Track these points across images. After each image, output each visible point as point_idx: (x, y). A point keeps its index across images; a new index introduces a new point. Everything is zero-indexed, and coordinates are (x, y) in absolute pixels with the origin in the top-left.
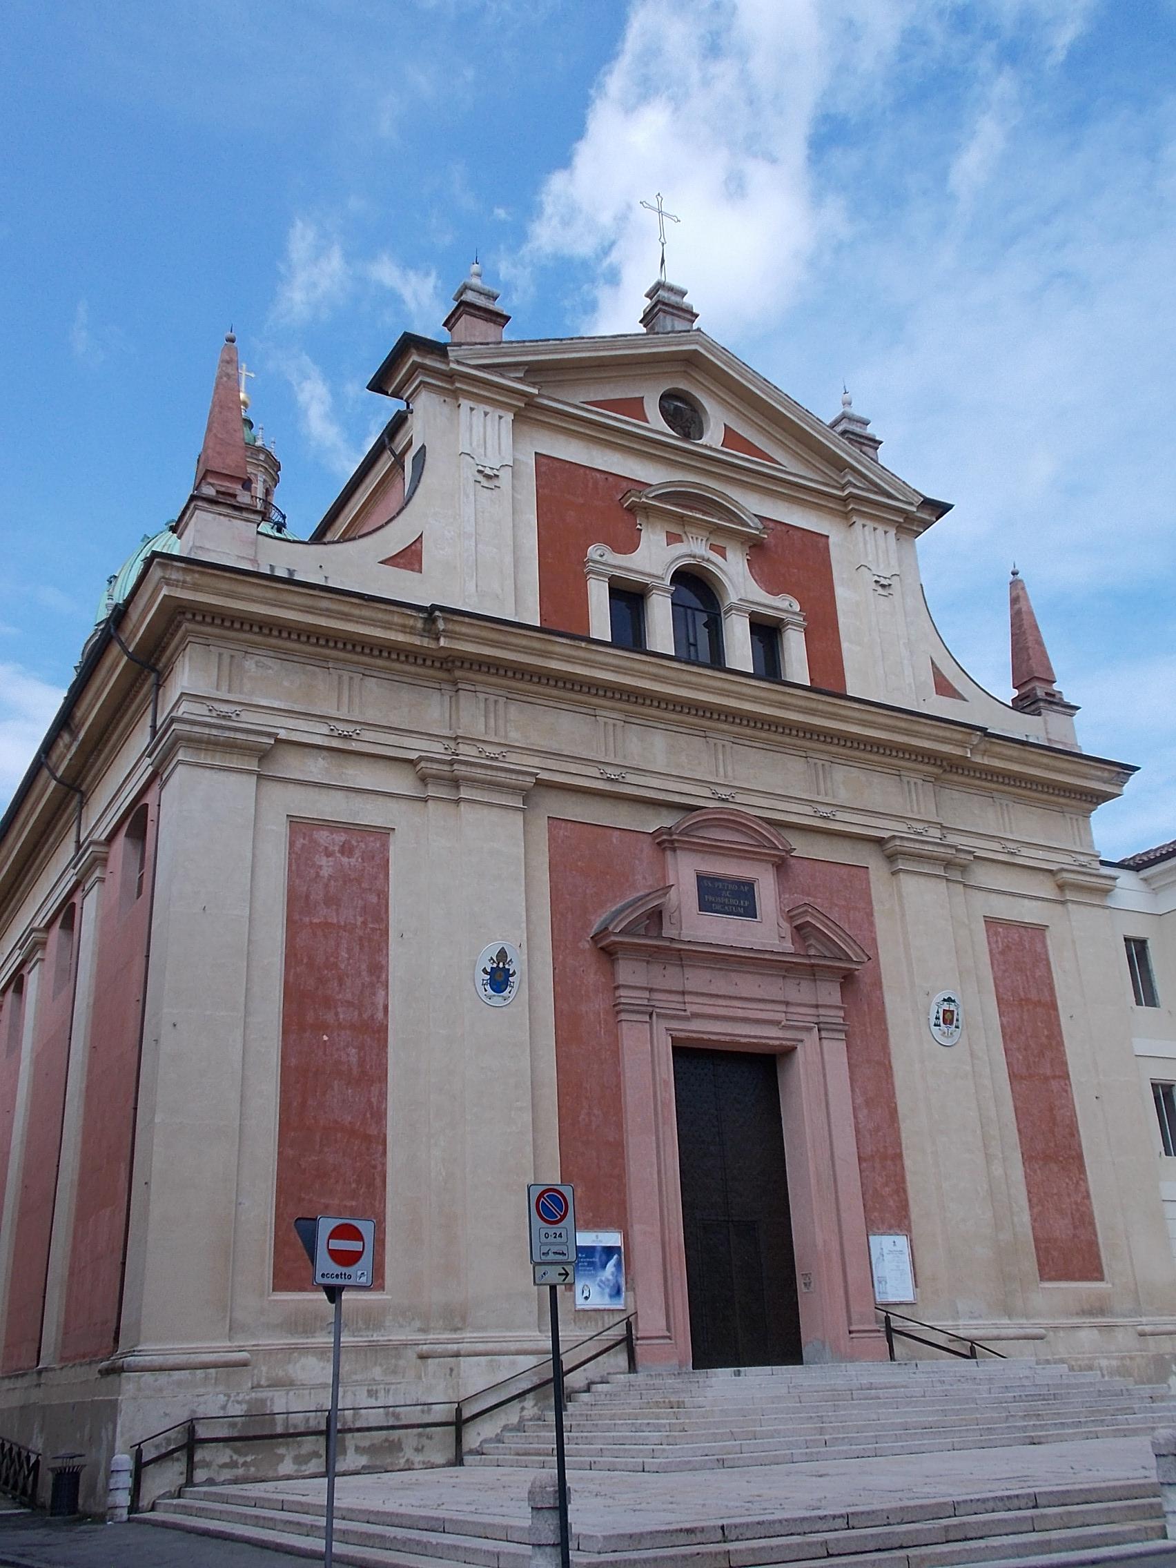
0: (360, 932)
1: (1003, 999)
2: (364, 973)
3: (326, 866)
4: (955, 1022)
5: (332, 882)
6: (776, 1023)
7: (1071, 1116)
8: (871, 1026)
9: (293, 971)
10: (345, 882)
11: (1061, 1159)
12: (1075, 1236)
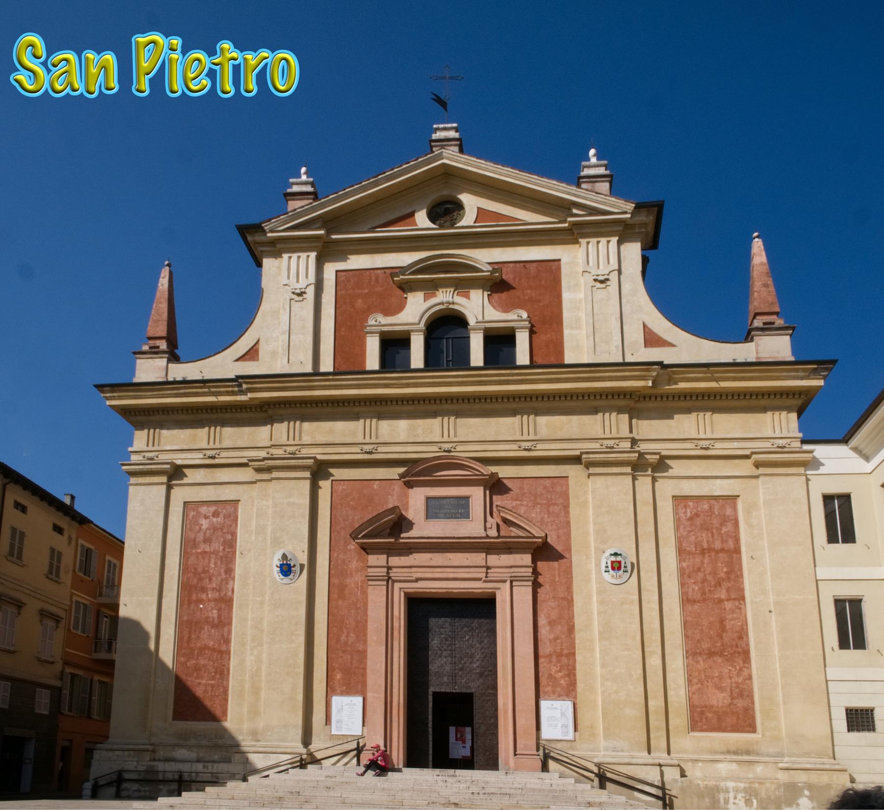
0: (221, 554)
1: (685, 550)
2: (223, 574)
3: (205, 524)
4: (623, 568)
5: (208, 532)
7: (742, 625)
8: (559, 576)
9: (186, 576)
10: (214, 531)
11: (726, 654)
12: (730, 704)
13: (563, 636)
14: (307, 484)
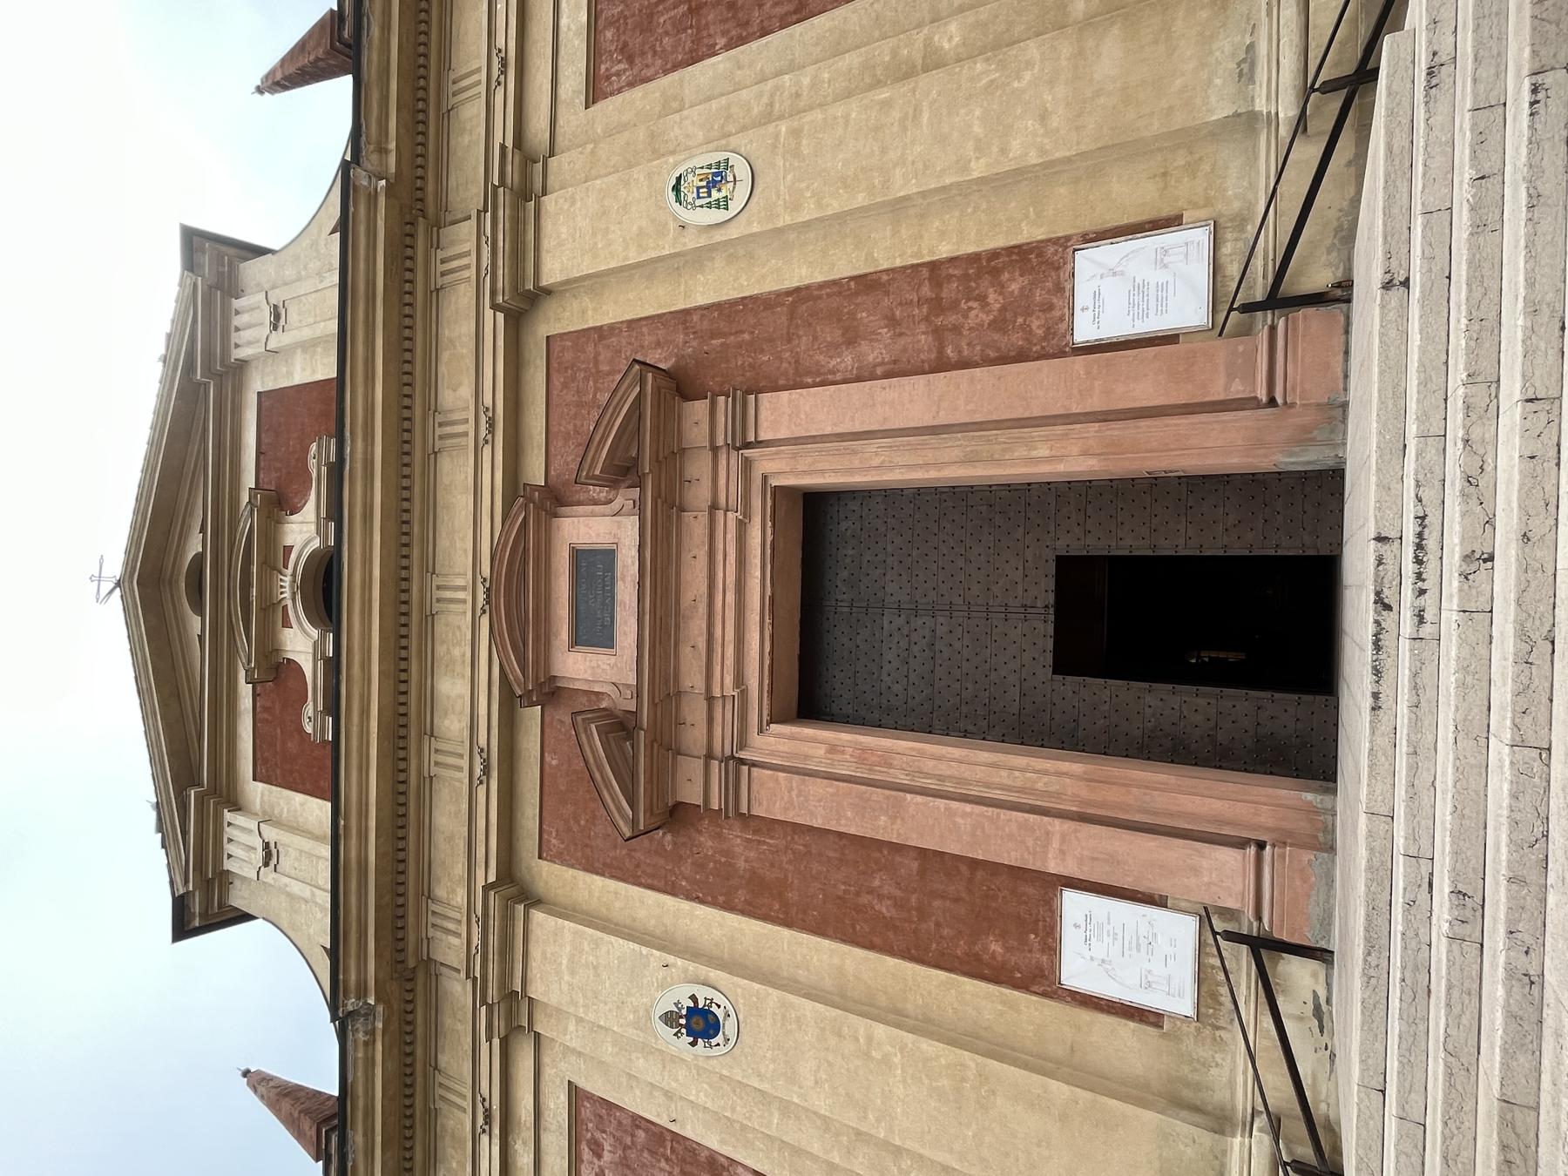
6: (742, 526)
13: (886, 302)
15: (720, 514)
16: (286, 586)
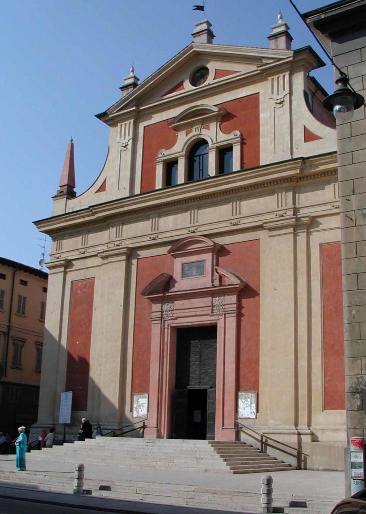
14: (124, 264)
15: (211, 308)
16: (195, 132)
